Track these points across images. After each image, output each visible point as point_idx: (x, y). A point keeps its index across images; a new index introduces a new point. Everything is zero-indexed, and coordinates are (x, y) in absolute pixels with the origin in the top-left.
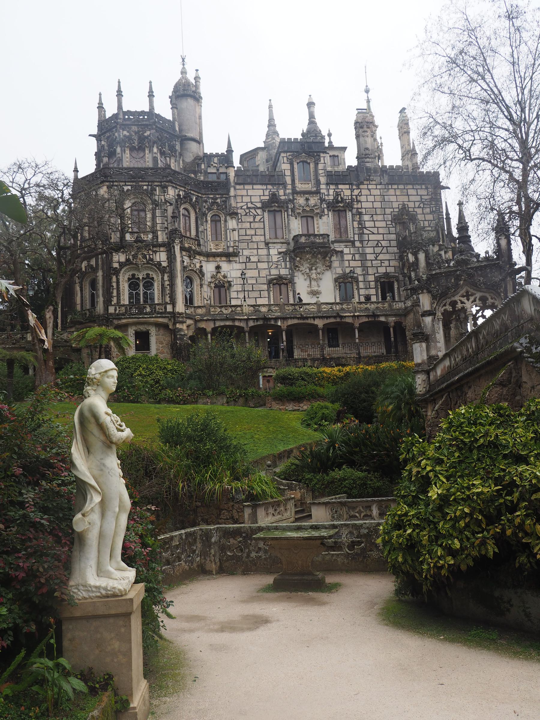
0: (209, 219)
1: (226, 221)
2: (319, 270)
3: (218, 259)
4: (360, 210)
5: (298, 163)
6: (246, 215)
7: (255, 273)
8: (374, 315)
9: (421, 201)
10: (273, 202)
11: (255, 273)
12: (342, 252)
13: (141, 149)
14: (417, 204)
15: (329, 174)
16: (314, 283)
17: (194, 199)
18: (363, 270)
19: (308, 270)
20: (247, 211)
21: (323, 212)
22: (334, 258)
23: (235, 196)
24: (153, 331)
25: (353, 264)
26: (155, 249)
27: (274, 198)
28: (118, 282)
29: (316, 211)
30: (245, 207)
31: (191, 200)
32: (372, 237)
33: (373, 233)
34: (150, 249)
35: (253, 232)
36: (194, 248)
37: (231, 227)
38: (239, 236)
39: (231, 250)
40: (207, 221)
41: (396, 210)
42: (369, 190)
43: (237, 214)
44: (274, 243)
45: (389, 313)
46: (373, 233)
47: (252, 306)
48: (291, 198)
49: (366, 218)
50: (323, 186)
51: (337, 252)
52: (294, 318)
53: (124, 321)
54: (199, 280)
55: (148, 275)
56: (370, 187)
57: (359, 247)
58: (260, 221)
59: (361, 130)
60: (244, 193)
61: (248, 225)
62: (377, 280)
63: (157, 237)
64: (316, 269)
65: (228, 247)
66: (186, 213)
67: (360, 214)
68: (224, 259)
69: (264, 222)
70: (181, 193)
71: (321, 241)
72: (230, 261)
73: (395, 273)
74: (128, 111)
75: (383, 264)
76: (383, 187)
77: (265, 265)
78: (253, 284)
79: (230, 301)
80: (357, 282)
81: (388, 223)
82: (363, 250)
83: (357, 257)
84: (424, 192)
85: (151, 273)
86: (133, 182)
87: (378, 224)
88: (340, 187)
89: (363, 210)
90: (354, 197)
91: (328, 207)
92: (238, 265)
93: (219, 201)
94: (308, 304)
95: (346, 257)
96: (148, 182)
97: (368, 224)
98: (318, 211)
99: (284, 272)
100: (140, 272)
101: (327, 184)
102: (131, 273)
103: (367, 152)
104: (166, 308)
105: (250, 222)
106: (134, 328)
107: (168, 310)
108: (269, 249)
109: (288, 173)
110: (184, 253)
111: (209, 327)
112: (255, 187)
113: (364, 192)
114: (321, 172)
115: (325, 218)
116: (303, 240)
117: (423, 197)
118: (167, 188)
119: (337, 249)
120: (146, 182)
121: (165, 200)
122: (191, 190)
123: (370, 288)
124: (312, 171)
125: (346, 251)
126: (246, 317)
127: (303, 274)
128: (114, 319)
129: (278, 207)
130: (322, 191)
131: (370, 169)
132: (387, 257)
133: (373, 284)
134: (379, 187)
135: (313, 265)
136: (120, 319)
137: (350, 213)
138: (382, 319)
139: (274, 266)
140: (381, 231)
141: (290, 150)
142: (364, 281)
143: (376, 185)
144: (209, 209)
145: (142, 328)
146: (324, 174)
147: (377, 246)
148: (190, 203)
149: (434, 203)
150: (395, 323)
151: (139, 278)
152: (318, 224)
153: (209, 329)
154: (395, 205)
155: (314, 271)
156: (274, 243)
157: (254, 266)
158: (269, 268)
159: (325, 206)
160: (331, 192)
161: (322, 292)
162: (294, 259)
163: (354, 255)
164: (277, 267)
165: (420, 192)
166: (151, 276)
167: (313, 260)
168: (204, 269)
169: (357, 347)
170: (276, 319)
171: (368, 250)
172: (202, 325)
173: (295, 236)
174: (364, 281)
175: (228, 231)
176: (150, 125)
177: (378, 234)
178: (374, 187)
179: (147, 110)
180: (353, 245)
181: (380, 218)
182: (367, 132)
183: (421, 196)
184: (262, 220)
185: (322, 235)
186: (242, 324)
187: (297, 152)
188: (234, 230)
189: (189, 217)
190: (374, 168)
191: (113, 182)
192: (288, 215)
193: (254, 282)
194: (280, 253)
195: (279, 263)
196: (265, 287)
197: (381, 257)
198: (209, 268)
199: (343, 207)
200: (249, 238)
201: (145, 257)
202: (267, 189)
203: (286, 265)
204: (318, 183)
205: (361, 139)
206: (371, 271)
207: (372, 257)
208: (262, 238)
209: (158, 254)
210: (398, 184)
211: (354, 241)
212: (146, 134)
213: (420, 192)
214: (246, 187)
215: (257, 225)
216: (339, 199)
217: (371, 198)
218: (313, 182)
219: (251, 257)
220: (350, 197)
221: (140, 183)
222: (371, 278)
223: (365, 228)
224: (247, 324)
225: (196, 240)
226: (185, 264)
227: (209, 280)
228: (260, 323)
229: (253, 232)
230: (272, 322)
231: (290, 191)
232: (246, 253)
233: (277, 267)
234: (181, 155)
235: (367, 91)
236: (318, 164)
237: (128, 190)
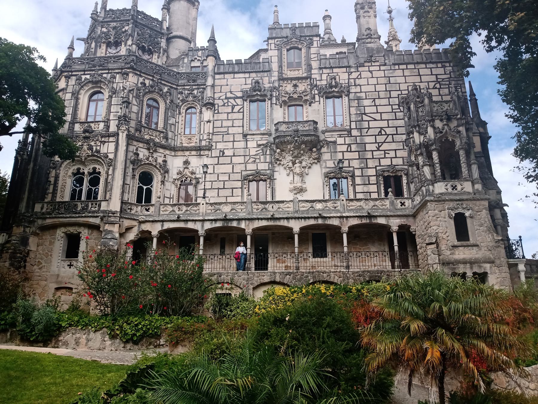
0: (183, 111)
1: (201, 112)
2: (304, 164)
3: (187, 153)
4: (358, 95)
5: (288, 50)
6: (224, 105)
7: (229, 169)
8: (370, 216)
9: (437, 81)
10: (255, 91)
11: (229, 169)
12: (335, 142)
13: (117, 44)
14: (432, 85)
15: (322, 57)
16: (297, 178)
17: (166, 89)
18: (360, 163)
19: (290, 164)
20: (226, 101)
21: (314, 98)
22: (324, 150)
23: (213, 86)
24: (85, 233)
25: (347, 155)
26: (103, 139)
27: (257, 86)
28: (57, 177)
29: (305, 98)
30: (224, 97)
31: (161, 90)
32: (373, 124)
33: (375, 120)
34: (97, 140)
35: (230, 123)
36: (157, 140)
37: (206, 119)
38: (214, 128)
39: (204, 143)
40: (180, 113)
41: (403, 92)
42: (371, 72)
43: (213, 105)
44: (253, 134)
45: (389, 213)
46: (375, 120)
47: (211, 204)
48: (276, 84)
49: (366, 102)
50: (313, 71)
51: (328, 143)
52: (262, 219)
53: (49, 221)
54: (160, 177)
55: (94, 169)
56: (372, 69)
57: (356, 137)
58: (239, 112)
59: (362, 11)
60: (224, 82)
61: (225, 116)
62: (377, 176)
63: (109, 127)
64: (301, 163)
65: (200, 140)
66: (155, 104)
67: (359, 99)
68: (194, 153)
69: (243, 112)
70: (147, 82)
71: (307, 128)
72: (200, 155)
73: (404, 165)
74: (110, 10)
75: (387, 155)
76: (389, 68)
77: (241, 160)
78: (224, 181)
79: (196, 200)
80: (353, 177)
81: (394, 107)
82: (361, 140)
83: (354, 147)
84: (441, 71)
85: (97, 167)
86: (93, 70)
87: (380, 109)
88: (335, 70)
89: (363, 95)
90: (352, 81)
91: (320, 93)
92: (210, 159)
93: (195, 92)
94: (282, 202)
95: (339, 148)
96: (109, 69)
97: (368, 110)
98: (308, 97)
99: (263, 167)
100: (85, 166)
101: (320, 68)
102: (76, 167)
103: (368, 32)
104: (100, 206)
105: (228, 113)
106: (63, 229)
107: (102, 209)
108: (247, 141)
109: (275, 60)
110: (141, 145)
111: (155, 229)
112: (236, 76)
113: (364, 75)
114: (312, 56)
115: (315, 106)
116: (283, 128)
117: (439, 77)
118: (127, 75)
119: (329, 140)
120: (105, 70)
121: (123, 87)
122: (161, 80)
123: (369, 184)
124: (303, 56)
125: (340, 141)
126: (201, 218)
127: (285, 168)
128: (38, 218)
129: (261, 96)
130: (313, 76)
131: (372, 49)
132: (394, 146)
133: (373, 180)
134: (382, 68)
135: (296, 157)
136: (45, 219)
137: (347, 98)
138: (382, 221)
139: (252, 160)
140: (385, 116)
141: (279, 36)
142: (362, 176)
143: (380, 66)
144: (183, 101)
145: (72, 230)
146: (316, 59)
147: (380, 134)
148: (157, 92)
149: (453, 83)
150: (401, 227)
151: (84, 173)
152: (307, 112)
153: (155, 233)
154: (404, 87)
155: (297, 165)
156: (253, 134)
157: (228, 160)
158: (246, 163)
159: (316, 92)
160: (324, 77)
161: (308, 189)
162: (275, 152)
163: (349, 145)
164: (255, 161)
165: (435, 71)
166: (97, 170)
167: (296, 152)
168: (170, 165)
169: (347, 257)
170: (239, 220)
171: (367, 140)
172: (146, 227)
173: (275, 125)
174: (362, 176)
175: (202, 123)
176: (129, 20)
177: (381, 120)
178: (378, 68)
179: (129, 7)
180: (349, 134)
181: (385, 102)
182: (368, 12)
183: (436, 75)
184: (242, 110)
185: (307, 122)
186: (197, 226)
187: (287, 37)
188: (209, 121)
189: (158, 109)
190: (377, 48)
191: (72, 72)
192: (271, 104)
193: (227, 179)
194: (259, 146)
195: (258, 157)
196: (239, 184)
197: (385, 147)
198: (176, 164)
199: (338, 92)
200: (226, 129)
201: (90, 148)
202: (249, 77)
203: (265, 158)
204: (310, 68)
205: (362, 20)
206: (371, 163)
207: (374, 147)
208: (240, 130)
209: (106, 144)
210: (407, 64)
211: (351, 129)
212: (123, 30)
213: (435, 71)
214: (226, 76)
215: (235, 116)
216: (334, 83)
217: (373, 81)
218: (304, 67)
219: (225, 151)
220: (347, 81)
221: (100, 72)
222: (372, 172)
223: (365, 114)
224: (203, 226)
225: (163, 132)
226: (141, 156)
227: (175, 176)
228: (219, 224)
229: (230, 123)
230: (235, 224)
231: (276, 78)
232: (220, 146)
233: (254, 162)
234: (165, 51)
235: (390, 12)
236: (310, 48)
237: (86, 79)
